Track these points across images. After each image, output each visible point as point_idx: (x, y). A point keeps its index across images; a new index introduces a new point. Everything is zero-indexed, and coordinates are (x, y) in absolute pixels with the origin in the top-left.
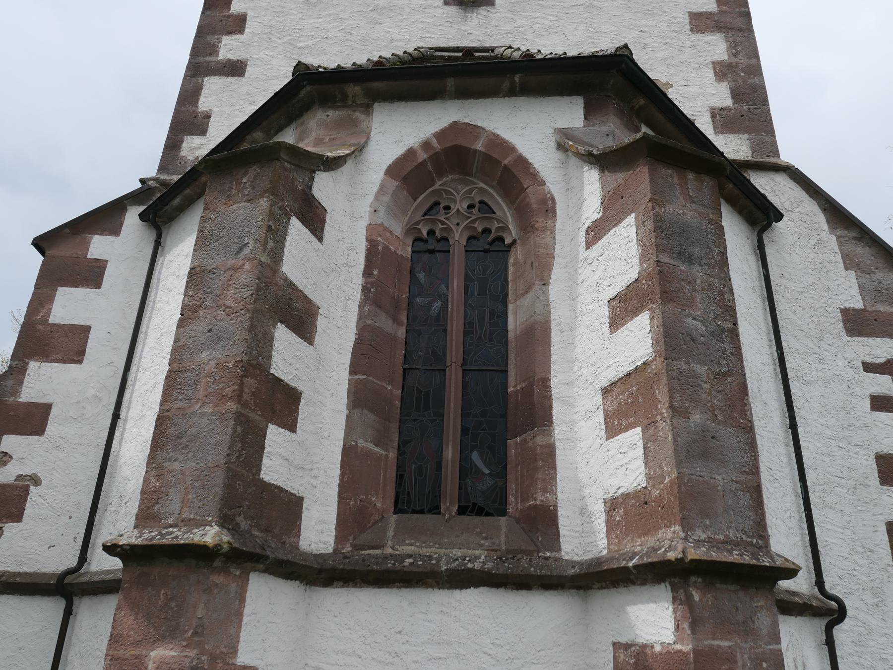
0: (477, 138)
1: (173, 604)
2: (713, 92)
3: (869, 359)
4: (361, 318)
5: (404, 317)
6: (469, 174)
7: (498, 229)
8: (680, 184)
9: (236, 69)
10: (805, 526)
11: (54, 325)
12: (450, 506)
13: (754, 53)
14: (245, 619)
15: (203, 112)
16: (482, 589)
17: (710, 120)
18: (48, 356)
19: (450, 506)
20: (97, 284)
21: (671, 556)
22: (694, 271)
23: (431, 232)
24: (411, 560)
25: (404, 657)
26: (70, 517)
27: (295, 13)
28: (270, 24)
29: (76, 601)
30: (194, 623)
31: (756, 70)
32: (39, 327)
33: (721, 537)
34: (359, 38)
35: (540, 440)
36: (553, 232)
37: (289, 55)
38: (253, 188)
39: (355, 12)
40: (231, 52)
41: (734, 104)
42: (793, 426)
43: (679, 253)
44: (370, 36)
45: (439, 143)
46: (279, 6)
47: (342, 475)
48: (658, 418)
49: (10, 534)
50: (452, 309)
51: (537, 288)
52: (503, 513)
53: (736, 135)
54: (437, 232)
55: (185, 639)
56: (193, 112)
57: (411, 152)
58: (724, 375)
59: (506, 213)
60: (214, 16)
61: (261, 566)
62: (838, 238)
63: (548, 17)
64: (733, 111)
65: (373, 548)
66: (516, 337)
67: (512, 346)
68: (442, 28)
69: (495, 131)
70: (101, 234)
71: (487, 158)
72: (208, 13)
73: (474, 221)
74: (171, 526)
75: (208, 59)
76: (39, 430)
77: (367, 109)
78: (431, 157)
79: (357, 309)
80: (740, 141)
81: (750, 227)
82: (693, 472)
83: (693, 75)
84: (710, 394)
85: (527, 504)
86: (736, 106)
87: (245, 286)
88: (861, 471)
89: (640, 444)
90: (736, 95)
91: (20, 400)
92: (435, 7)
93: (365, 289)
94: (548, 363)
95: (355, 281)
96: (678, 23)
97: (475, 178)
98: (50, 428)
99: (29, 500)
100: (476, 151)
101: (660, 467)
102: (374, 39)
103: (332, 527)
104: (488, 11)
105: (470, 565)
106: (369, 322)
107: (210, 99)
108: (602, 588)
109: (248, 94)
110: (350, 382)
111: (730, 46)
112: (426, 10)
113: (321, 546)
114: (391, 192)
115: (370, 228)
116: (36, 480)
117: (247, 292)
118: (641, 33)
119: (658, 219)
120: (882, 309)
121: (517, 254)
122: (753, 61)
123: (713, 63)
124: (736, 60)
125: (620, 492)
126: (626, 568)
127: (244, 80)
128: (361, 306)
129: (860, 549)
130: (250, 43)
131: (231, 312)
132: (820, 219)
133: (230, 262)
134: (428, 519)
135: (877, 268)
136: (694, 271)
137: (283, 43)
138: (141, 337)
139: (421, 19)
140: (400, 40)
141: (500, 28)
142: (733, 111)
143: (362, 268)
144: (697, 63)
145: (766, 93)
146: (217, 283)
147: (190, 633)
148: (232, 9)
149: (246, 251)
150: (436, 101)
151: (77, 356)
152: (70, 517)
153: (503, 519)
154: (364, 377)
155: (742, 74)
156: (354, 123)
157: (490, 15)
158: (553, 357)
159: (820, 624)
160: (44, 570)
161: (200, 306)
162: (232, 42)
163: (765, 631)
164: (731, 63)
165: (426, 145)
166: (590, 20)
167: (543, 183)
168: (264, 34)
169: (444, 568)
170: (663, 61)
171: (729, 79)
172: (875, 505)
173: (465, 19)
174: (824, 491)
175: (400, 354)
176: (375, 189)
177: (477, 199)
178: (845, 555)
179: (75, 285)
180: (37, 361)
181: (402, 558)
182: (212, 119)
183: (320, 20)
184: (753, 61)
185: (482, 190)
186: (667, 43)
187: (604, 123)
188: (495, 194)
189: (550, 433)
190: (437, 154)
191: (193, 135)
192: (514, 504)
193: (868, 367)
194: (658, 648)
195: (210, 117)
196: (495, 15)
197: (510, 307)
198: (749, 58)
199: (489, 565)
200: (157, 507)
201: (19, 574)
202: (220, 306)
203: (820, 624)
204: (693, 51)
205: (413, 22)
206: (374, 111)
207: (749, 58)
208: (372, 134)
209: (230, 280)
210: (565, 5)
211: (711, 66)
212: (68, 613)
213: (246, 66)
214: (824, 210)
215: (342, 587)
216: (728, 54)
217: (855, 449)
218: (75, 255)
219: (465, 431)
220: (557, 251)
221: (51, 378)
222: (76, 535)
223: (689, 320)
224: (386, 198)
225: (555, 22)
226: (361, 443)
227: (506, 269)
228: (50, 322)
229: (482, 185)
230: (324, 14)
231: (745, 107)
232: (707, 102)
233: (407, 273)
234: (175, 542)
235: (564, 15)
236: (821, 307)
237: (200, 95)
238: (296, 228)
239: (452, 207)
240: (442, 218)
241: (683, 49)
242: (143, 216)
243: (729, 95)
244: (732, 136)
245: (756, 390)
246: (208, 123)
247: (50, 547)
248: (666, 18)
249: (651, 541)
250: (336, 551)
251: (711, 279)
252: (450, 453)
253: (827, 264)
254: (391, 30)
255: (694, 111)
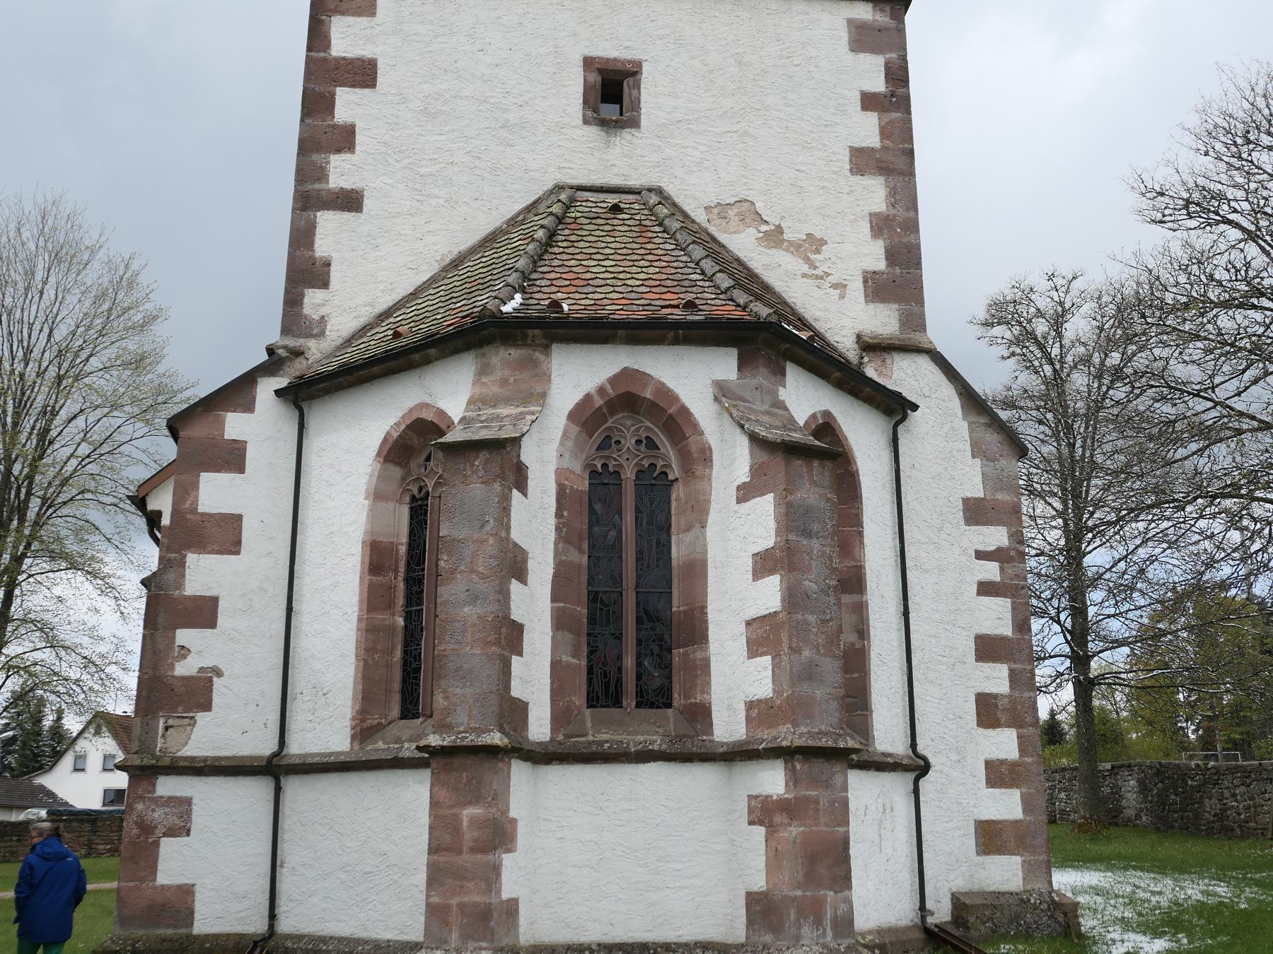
0: (645, 385)
1: (474, 782)
2: (867, 251)
3: (981, 548)
4: (556, 554)
5: (586, 546)
6: (638, 414)
7: (662, 466)
8: (808, 473)
9: (350, 201)
10: (907, 699)
11: (203, 514)
12: (629, 701)
13: (913, 205)
14: (511, 789)
15: (321, 258)
16: (659, 763)
17: (862, 285)
18: (205, 548)
19: (629, 701)
20: (241, 469)
21: (784, 744)
22: (812, 544)
23: (605, 466)
24: (608, 745)
25: (607, 810)
26: (257, 705)
27: (413, 125)
28: (384, 140)
29: (282, 780)
30: (492, 792)
31: (912, 226)
32: (190, 516)
33: (816, 730)
34: (489, 164)
35: (699, 655)
36: (710, 480)
37: (411, 185)
38: (486, 471)
39: (482, 129)
40: (343, 177)
41: (888, 266)
42: (906, 614)
43: (803, 531)
44: (501, 162)
45: (612, 389)
46: (393, 115)
47: (552, 683)
48: (782, 653)
49: (203, 723)
50: (626, 539)
51: (697, 529)
52: (669, 705)
53: (887, 305)
54: (610, 466)
55: (487, 803)
56: (310, 257)
57: (588, 398)
58: (827, 620)
59: (667, 448)
60: (316, 126)
61: (517, 755)
62: (970, 424)
63: (699, 146)
64: (885, 276)
65: (579, 736)
66: (679, 566)
67: (675, 572)
68: (582, 156)
69: (661, 379)
70: (235, 411)
71: (654, 405)
72: (308, 121)
73: (643, 459)
74: (463, 732)
75: (317, 186)
76: (211, 623)
77: (546, 348)
78: (606, 403)
79: (553, 546)
80: (889, 312)
81: (887, 418)
82: (801, 689)
83: (848, 229)
84: (816, 635)
85: (689, 701)
86: (890, 269)
87: (491, 557)
88: (961, 650)
89: (770, 668)
90: (892, 256)
91: (186, 593)
92: (573, 127)
93: (558, 529)
94: (705, 594)
95: (549, 521)
96: (838, 161)
97: (643, 416)
98: (221, 620)
99: (214, 691)
100: (645, 398)
101: (782, 686)
102: (506, 168)
103: (548, 721)
104: (633, 135)
105: (650, 747)
106: (564, 558)
107: (326, 241)
108: (741, 760)
109: (369, 235)
110: (552, 608)
111: (890, 192)
112: (563, 131)
113: (541, 736)
114: (573, 437)
115: (558, 472)
116: (219, 673)
117: (494, 563)
118: (797, 172)
119: (789, 505)
120: (1000, 497)
121: (678, 493)
122: (911, 214)
123: (870, 215)
124: (894, 212)
125: (756, 698)
126: (757, 750)
127: (363, 216)
128: (556, 544)
129: (951, 716)
130: (364, 167)
131: (484, 577)
132: (955, 403)
133: (476, 536)
134: (614, 712)
135: (1001, 456)
136: (812, 544)
137: (402, 168)
138: (299, 526)
139: (559, 143)
140: (536, 171)
141: (646, 159)
142: (885, 276)
143: (554, 509)
144: (854, 215)
145: (920, 254)
146: (467, 553)
147: (490, 799)
148: (336, 116)
149: (488, 528)
150: (608, 345)
151: (233, 545)
152: (257, 705)
153: (670, 711)
154: (563, 605)
155: (899, 230)
156: (535, 364)
157: (635, 140)
158: (709, 589)
159: (910, 777)
160: (241, 754)
161: (455, 569)
162: (342, 164)
163: (839, 785)
164: (889, 215)
165: (601, 390)
166: (745, 153)
167: (702, 433)
168: (379, 154)
169: (633, 750)
170: (818, 211)
171: (885, 236)
172: (969, 679)
173: (608, 144)
174: (928, 668)
175: (585, 577)
176: (560, 434)
177: (644, 436)
178: (939, 721)
179: (218, 469)
180: (194, 553)
181: (601, 743)
182: (333, 268)
183: (442, 138)
184: (911, 214)
185: (648, 428)
186: (824, 187)
187: (754, 376)
188: (660, 433)
189: (707, 649)
190: (611, 399)
191: (313, 288)
192: (677, 700)
193: (980, 555)
194: (775, 797)
195: (329, 265)
196: (640, 141)
197: (674, 538)
198: (908, 210)
199: (664, 747)
200: (448, 719)
201: (220, 758)
202: (472, 571)
203: (910, 777)
204: (851, 199)
205: (549, 146)
206: (553, 352)
207: (908, 210)
208: (552, 377)
209: (478, 551)
210: (717, 130)
211: (867, 219)
212: (278, 790)
213: (362, 197)
214: (960, 395)
215: (559, 764)
216: (887, 203)
217: (958, 631)
218: (211, 436)
219: (639, 642)
220: (713, 498)
221: (212, 570)
222: (265, 721)
223: (806, 583)
224: (570, 444)
225: (706, 154)
226: (565, 658)
227: (669, 502)
228: (199, 511)
229: (648, 424)
230: (446, 129)
231: (898, 270)
232: (861, 264)
233: (586, 506)
234: (473, 743)
235: (716, 144)
236: (945, 497)
237: (315, 235)
238: (515, 492)
239: (623, 442)
240: (615, 456)
241: (840, 195)
242: (279, 393)
243: (883, 256)
244: (882, 305)
245: (874, 586)
246: (329, 272)
247: (243, 733)
248: (825, 154)
249: (774, 732)
250: (552, 740)
251: (824, 548)
252: (629, 662)
253: (955, 453)
254: (524, 155)
255: (846, 275)
